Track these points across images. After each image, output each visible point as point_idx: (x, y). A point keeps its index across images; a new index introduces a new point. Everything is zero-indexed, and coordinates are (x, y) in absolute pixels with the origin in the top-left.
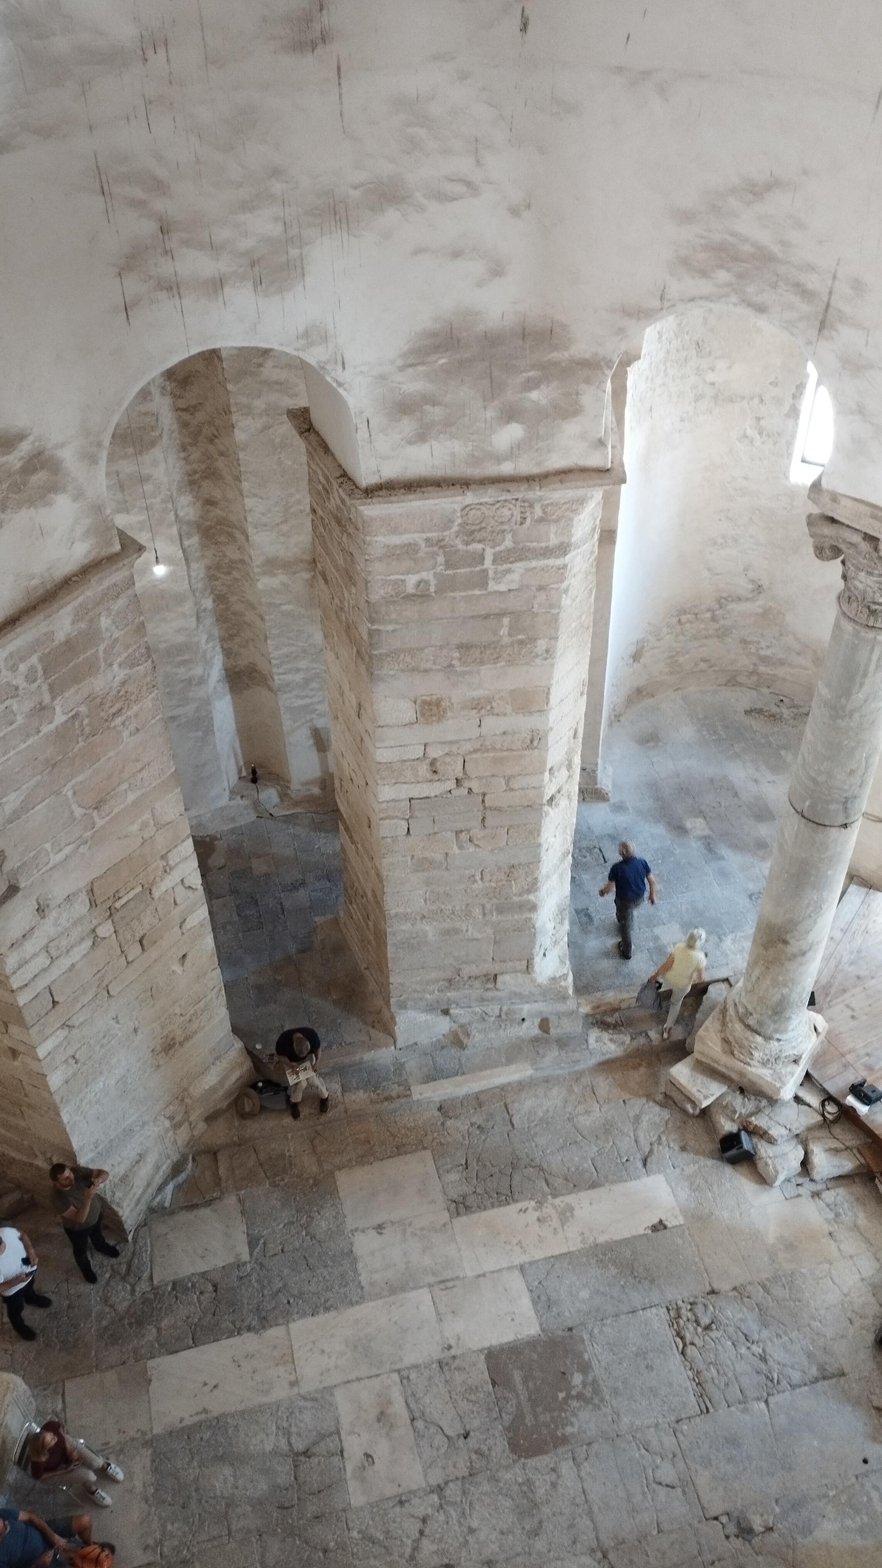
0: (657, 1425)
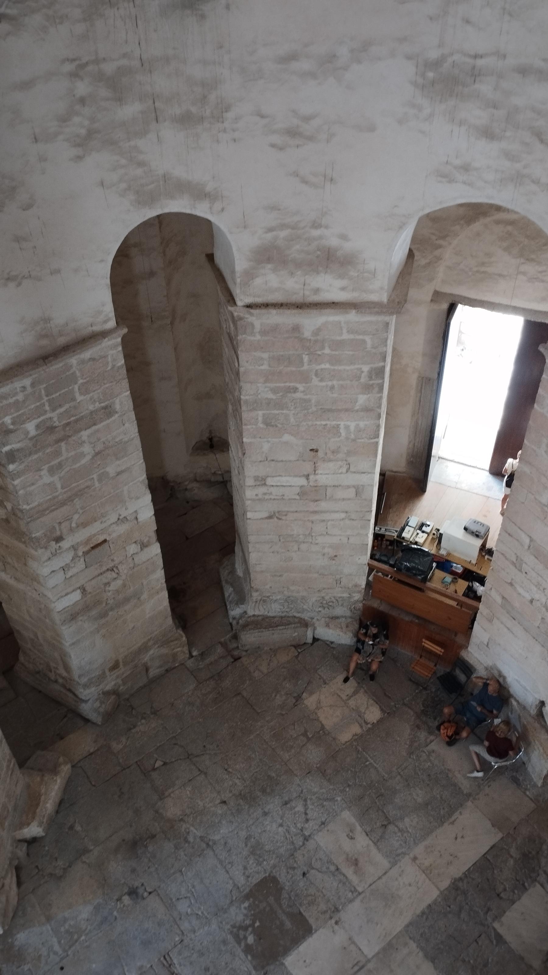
0: (194, 932)
